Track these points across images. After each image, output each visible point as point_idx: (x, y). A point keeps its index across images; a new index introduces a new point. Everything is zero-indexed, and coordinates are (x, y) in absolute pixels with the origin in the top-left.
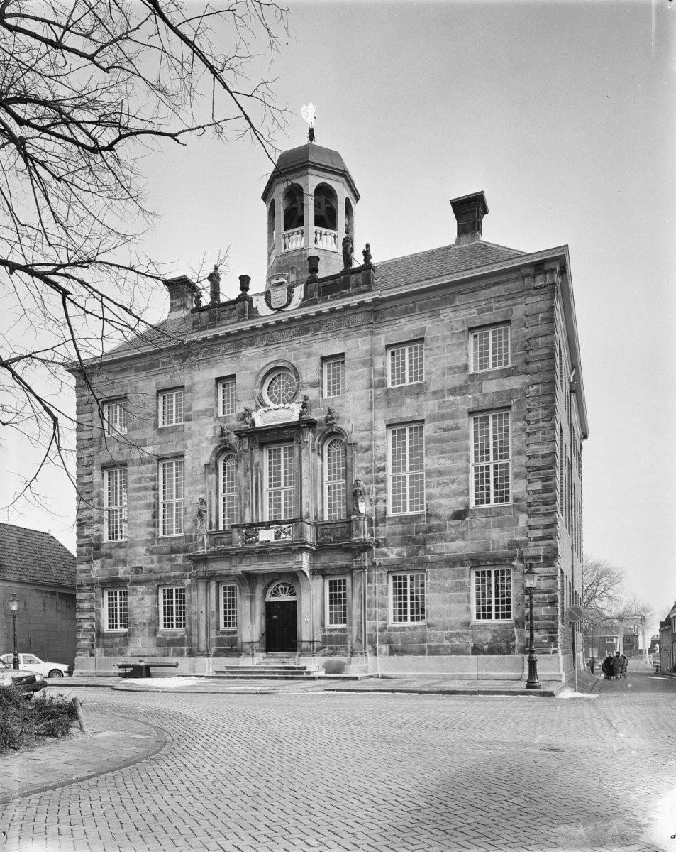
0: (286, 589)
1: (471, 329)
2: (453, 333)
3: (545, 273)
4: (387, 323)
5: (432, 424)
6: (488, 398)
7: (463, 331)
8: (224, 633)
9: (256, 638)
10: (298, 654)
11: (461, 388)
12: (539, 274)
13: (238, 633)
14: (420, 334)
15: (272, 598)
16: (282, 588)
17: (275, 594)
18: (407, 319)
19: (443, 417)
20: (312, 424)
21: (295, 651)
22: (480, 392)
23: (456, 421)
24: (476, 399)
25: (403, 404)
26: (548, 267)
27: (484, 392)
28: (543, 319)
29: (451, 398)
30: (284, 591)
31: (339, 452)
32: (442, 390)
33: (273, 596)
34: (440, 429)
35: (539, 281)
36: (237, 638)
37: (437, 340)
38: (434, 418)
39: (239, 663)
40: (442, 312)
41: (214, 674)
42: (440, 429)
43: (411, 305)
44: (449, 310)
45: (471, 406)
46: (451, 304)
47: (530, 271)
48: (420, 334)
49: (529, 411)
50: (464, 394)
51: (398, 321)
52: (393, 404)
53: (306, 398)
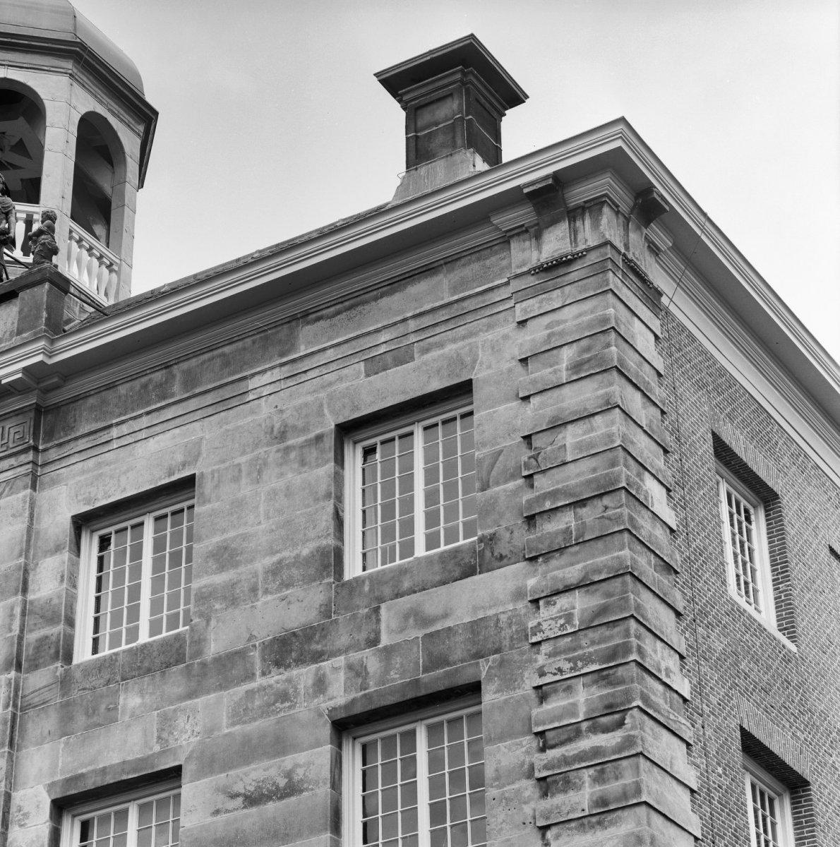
1: (347, 431)
2: (288, 450)
3: (574, 214)
4: (82, 444)
5: (205, 782)
6: (397, 660)
7: (319, 438)
11: (308, 633)
12: (554, 222)
14: (184, 465)
18: (145, 421)
19: (248, 751)
22: (373, 642)
23: (288, 761)
24: (358, 671)
25: (111, 716)
26: (580, 194)
27: (385, 640)
28: (576, 367)
29: (276, 679)
32: (241, 654)
34: (234, 796)
35: (555, 242)
37: (236, 479)
38: (211, 763)
40: (252, 384)
42: (234, 796)
43: (158, 376)
44: (277, 374)
45: (340, 695)
46: (282, 355)
47: (523, 215)
48: (184, 465)
49: (542, 693)
50: (318, 657)
51: (115, 432)
52: (81, 720)
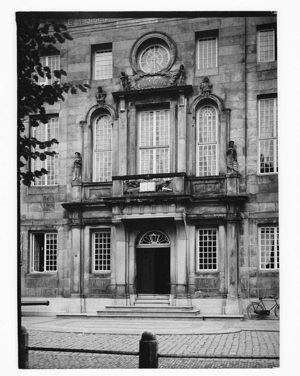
0: (157, 237)
8: (96, 275)
9: (131, 281)
10: (171, 296)
13: (112, 275)
15: (143, 244)
16: (153, 237)
17: (146, 241)
20: (188, 91)
21: (170, 293)
30: (154, 239)
31: (210, 118)
33: (144, 243)
36: (110, 281)
39: (116, 302)
41: (96, 314)
53: (182, 67)
